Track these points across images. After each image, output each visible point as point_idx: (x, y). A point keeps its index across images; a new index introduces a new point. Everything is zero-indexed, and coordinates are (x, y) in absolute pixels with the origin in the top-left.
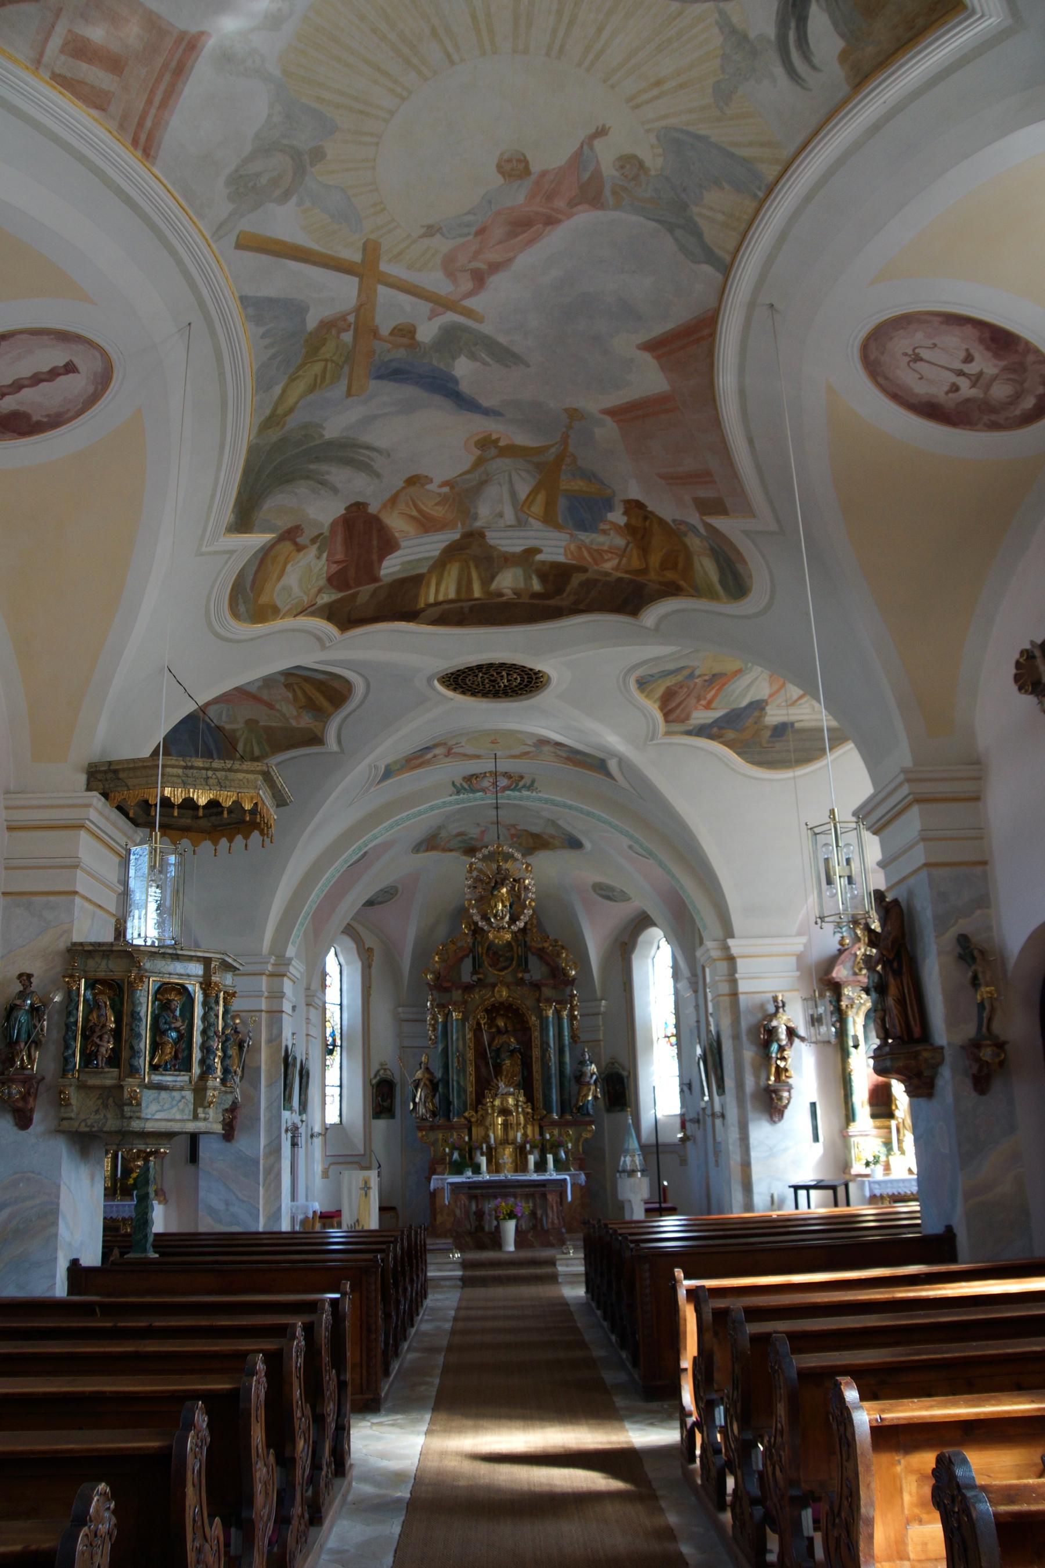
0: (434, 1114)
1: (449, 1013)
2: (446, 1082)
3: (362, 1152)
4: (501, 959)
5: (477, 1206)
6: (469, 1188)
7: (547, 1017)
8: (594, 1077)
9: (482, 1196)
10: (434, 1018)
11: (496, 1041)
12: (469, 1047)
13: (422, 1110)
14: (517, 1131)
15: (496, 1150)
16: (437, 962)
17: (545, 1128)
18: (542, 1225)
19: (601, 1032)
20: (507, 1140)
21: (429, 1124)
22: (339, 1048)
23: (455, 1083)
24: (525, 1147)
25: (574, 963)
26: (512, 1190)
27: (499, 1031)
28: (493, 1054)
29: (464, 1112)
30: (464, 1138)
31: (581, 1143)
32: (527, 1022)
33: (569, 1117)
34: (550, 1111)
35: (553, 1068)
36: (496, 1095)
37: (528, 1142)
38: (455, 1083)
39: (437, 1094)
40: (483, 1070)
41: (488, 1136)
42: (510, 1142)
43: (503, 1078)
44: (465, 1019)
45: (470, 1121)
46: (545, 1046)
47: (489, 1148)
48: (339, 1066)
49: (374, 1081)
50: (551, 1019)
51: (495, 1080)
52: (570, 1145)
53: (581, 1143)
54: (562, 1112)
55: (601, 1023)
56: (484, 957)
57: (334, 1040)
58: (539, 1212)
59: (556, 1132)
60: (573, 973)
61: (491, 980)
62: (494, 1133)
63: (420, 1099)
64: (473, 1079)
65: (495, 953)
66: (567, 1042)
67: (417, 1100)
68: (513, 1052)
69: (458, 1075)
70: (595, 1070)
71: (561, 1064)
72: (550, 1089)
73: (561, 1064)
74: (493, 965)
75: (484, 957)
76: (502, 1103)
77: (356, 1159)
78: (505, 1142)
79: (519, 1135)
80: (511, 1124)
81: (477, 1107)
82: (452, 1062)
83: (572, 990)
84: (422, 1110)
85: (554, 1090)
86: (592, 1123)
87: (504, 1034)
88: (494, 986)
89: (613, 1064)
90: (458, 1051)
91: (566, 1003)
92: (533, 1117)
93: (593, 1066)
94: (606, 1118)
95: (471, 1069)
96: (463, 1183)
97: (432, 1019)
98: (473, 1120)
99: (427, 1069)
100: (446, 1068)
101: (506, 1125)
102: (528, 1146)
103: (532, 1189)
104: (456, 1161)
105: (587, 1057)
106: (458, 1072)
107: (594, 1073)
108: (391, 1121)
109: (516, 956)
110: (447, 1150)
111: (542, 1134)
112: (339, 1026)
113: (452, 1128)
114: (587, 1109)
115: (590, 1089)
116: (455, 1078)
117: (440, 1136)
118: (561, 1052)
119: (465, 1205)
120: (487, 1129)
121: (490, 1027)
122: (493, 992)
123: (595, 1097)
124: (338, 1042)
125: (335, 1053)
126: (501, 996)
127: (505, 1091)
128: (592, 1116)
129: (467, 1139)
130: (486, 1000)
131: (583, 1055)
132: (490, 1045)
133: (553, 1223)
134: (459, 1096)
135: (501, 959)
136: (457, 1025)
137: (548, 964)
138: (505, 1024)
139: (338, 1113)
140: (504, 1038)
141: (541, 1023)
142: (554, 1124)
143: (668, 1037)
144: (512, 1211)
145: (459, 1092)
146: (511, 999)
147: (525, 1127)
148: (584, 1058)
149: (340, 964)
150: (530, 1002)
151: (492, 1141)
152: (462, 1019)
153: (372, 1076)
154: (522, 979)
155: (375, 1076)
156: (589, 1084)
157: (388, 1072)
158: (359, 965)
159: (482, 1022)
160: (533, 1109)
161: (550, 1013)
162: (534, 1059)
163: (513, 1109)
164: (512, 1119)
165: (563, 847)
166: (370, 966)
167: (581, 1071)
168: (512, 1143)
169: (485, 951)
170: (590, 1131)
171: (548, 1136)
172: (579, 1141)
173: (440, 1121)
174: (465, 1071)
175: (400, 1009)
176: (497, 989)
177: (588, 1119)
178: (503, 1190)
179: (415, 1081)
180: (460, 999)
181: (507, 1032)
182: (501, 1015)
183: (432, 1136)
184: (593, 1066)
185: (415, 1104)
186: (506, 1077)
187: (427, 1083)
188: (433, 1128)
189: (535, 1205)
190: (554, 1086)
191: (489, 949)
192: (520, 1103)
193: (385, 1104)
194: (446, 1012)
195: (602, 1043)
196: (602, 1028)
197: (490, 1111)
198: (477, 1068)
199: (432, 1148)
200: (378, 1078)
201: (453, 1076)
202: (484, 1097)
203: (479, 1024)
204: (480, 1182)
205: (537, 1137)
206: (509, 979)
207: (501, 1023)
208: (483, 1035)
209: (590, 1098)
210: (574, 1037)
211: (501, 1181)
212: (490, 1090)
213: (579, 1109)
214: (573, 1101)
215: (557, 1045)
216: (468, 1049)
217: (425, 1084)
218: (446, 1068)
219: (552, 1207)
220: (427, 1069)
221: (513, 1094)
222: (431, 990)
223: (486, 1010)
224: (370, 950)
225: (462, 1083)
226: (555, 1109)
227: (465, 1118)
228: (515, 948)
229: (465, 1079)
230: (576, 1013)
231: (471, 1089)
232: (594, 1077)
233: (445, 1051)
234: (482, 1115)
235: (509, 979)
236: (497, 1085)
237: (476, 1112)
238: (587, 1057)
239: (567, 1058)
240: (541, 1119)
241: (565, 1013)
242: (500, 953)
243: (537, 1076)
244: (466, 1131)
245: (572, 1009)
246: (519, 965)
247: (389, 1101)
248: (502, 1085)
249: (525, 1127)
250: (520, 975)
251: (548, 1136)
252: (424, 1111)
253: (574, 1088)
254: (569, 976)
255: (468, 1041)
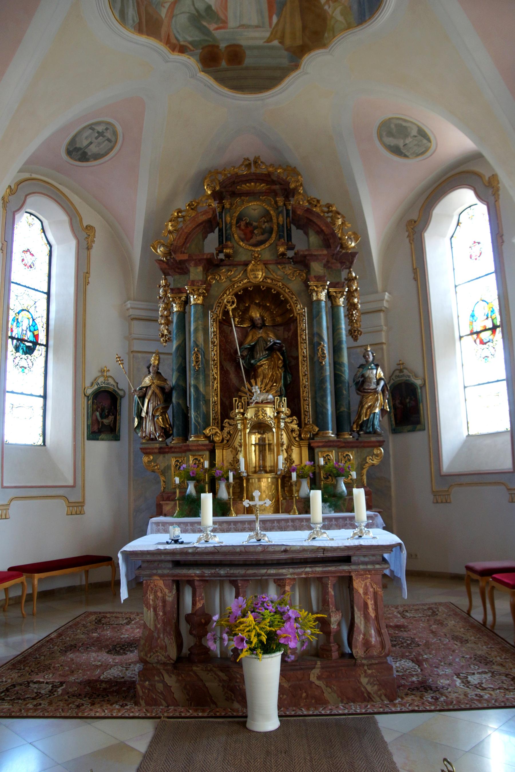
0: (166, 433)
1: (187, 302)
2: (184, 393)
3: (71, 483)
4: (256, 232)
5: (194, 603)
6: (177, 564)
7: (319, 301)
8: (382, 383)
9: (205, 581)
10: (168, 308)
11: (250, 338)
12: (213, 343)
13: (149, 427)
14: (278, 455)
15: (248, 480)
16: (170, 232)
17: (316, 450)
18: (340, 646)
19: (383, 334)
20: (264, 467)
21: (157, 445)
22: (43, 348)
23: (192, 390)
24: (290, 477)
25: (354, 233)
26: (272, 571)
27: (254, 326)
28: (245, 353)
29: (204, 429)
30: (203, 464)
31: (365, 471)
32: (291, 311)
33: (347, 436)
34: (323, 427)
35: (328, 368)
36: (248, 404)
37: (294, 470)
38: (192, 390)
39: (171, 405)
40: (232, 376)
41: (238, 461)
42: (268, 469)
43: (259, 383)
44: (206, 307)
45: (213, 442)
46: (316, 339)
47: (238, 477)
48: (43, 369)
49: (89, 391)
50: (323, 304)
51: (247, 385)
52: (354, 474)
53: (365, 471)
54: (339, 430)
55: (383, 322)
56: (234, 229)
57: (36, 337)
58: (335, 618)
59: (333, 456)
60: (353, 244)
61: (243, 257)
62: (245, 457)
63: (147, 413)
64: (217, 385)
65: (247, 225)
66: (344, 337)
67: (143, 415)
68: (271, 350)
69: (197, 378)
70: (382, 375)
71: (337, 365)
72: (324, 397)
73: (337, 365)
74: (246, 239)
75: (234, 229)
76: (256, 415)
77: (61, 492)
78: (262, 469)
79: (281, 459)
80: (270, 445)
81: (222, 422)
82: (190, 362)
83: (350, 272)
84: (149, 427)
85: (329, 399)
86: (380, 444)
87: (261, 328)
88: (246, 264)
89: (401, 371)
90: (197, 346)
91: (343, 287)
92: (300, 436)
93: (379, 370)
94: (392, 440)
95: (215, 372)
96: (159, 553)
97: (165, 309)
98: (217, 439)
99: (158, 374)
100: (182, 371)
101: (262, 446)
102: (294, 475)
103: (319, 569)
104: (190, 496)
105: (371, 358)
106: (197, 372)
107: (381, 379)
108: (114, 443)
109: (275, 227)
110: (177, 480)
111: (312, 457)
112: (45, 320)
113: (187, 450)
114: (373, 425)
115: (377, 400)
116: (192, 382)
117: (173, 462)
118: (336, 349)
119: (164, 601)
120: (237, 452)
121: (241, 322)
122: (246, 271)
123: (383, 410)
124: (42, 339)
125: (36, 353)
126: (256, 277)
127: (262, 398)
128: (379, 435)
129: (206, 465)
130: (237, 282)
131: (365, 356)
132: (241, 345)
133: (367, 644)
134: (197, 407)
135: (256, 232)
136: (195, 312)
137: (320, 232)
138: (262, 317)
139: (40, 431)
140: (261, 333)
141: (310, 312)
142: (329, 444)
143: (478, 333)
144: (272, 636)
145: (197, 401)
146: (269, 281)
147: (289, 450)
148: (367, 361)
149: (49, 243)
150: (295, 285)
151: (243, 468)
152: (203, 305)
153: (88, 384)
154: (283, 254)
155: (92, 384)
156: (375, 391)
157: (111, 381)
158: (73, 243)
159: (230, 308)
160: (299, 425)
161: (323, 295)
162: (300, 358)
163: (272, 423)
164: (271, 437)
165: (349, 27)
166: (89, 248)
167: (363, 376)
168: (271, 472)
169: (234, 222)
170: (377, 455)
171: (322, 462)
172: (363, 469)
173: (174, 441)
174: (206, 377)
175: (129, 304)
176: (250, 267)
177: (373, 439)
178: (251, 571)
179: (141, 389)
180: (201, 277)
181: (263, 325)
182: (256, 304)
183: (162, 461)
184: (379, 370)
185: (141, 419)
186: (262, 382)
187: (157, 391)
188: (163, 451)
189: (324, 602)
190: (329, 391)
191: (239, 219)
192: (282, 416)
193: (106, 421)
194: (183, 298)
195: (385, 347)
196: (385, 328)
197: (239, 426)
198: (224, 373)
199: (162, 478)
200: (96, 387)
201: (191, 381)
202: (232, 408)
203: (226, 313)
204: (196, 552)
205: (306, 461)
206: (267, 256)
207: (256, 314)
208: (232, 331)
209: (377, 410)
210: (353, 333)
211: (244, 550)
212: (240, 397)
213: (362, 426)
214: (354, 418)
215: (331, 340)
216: (211, 345)
217: (153, 392)
218: (182, 371)
219: (366, 605)
220: (158, 374)
221: (273, 403)
222: (166, 274)
223: (236, 295)
224: (89, 228)
225: (201, 389)
226: (330, 426)
227: (206, 437)
228: (274, 219)
229: (206, 383)
230: (356, 300)
231: (215, 398)
232: (382, 383)
233: (182, 350)
234: (229, 433)
235: (267, 256)
236: (250, 391)
237: (222, 429)
238: (371, 358)
239: (345, 359)
240: (310, 439)
241: (341, 301)
242: (255, 224)
243: (305, 381)
244: (207, 453)
245: (350, 294)
246: (280, 237)
247: (111, 418)
248: (256, 389)
249: (289, 450)
250: (281, 250)
251: (322, 462)
252: (152, 428)
253: (355, 398)
254: (347, 248)
255: (211, 336)
